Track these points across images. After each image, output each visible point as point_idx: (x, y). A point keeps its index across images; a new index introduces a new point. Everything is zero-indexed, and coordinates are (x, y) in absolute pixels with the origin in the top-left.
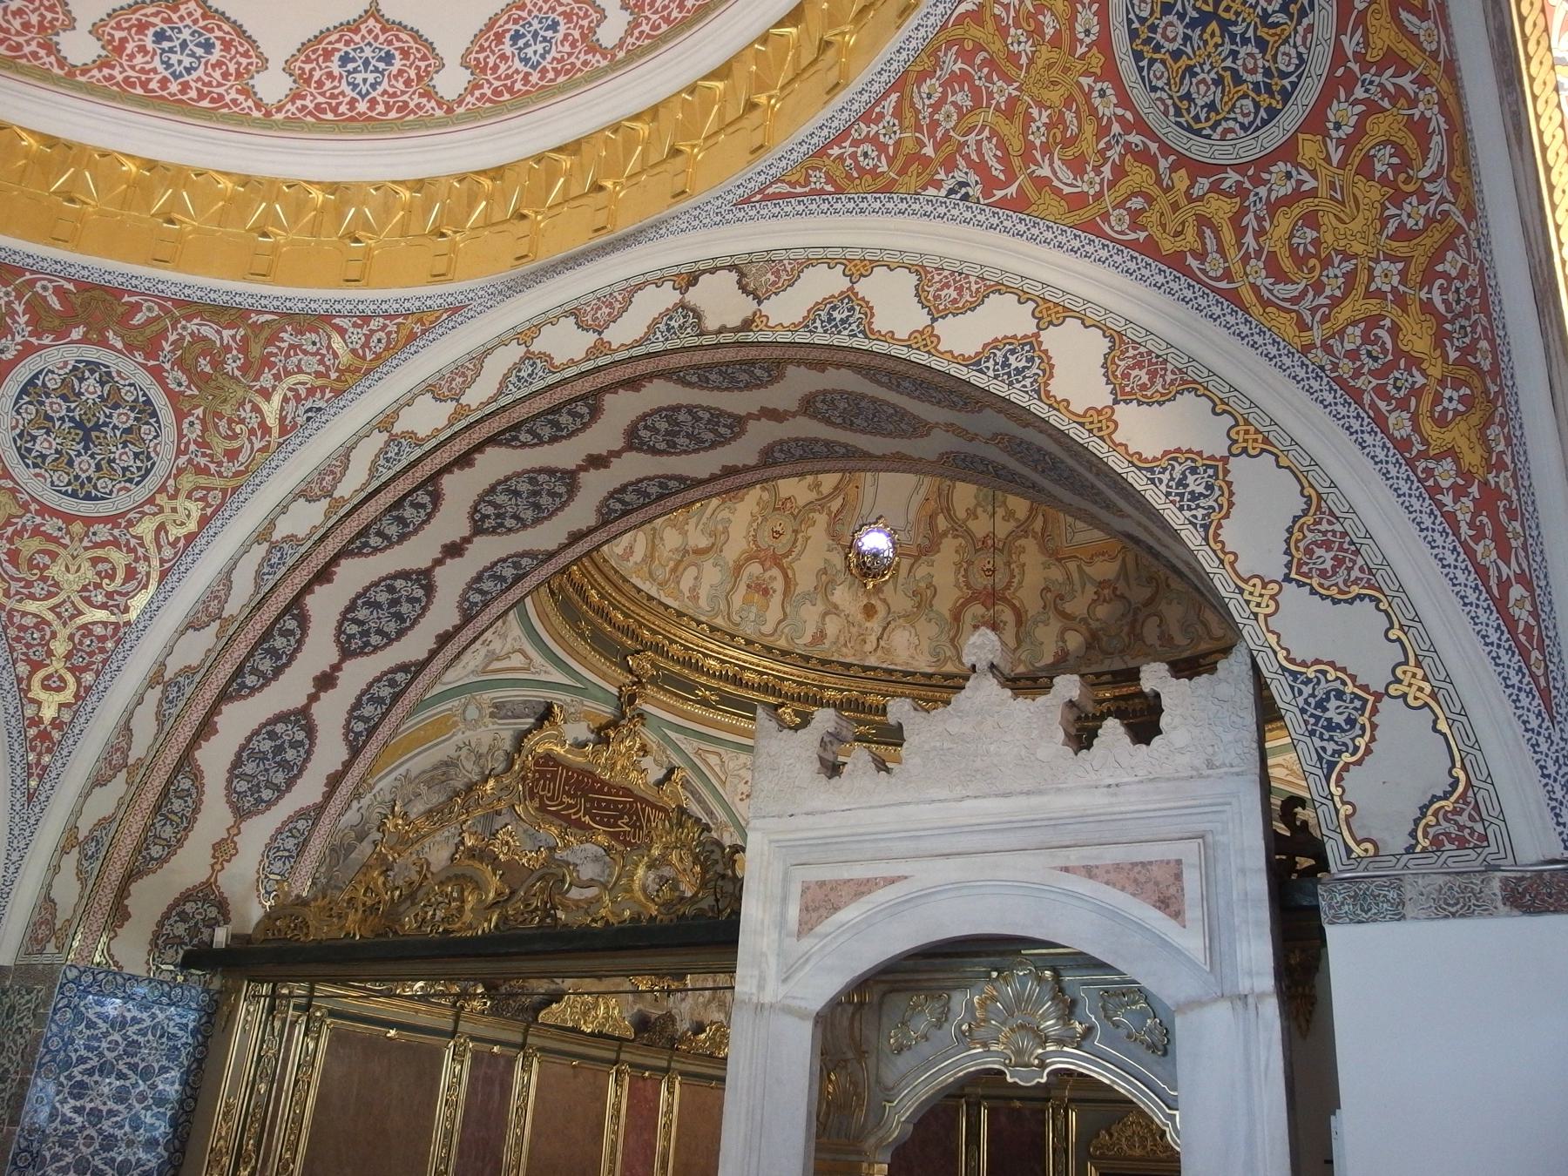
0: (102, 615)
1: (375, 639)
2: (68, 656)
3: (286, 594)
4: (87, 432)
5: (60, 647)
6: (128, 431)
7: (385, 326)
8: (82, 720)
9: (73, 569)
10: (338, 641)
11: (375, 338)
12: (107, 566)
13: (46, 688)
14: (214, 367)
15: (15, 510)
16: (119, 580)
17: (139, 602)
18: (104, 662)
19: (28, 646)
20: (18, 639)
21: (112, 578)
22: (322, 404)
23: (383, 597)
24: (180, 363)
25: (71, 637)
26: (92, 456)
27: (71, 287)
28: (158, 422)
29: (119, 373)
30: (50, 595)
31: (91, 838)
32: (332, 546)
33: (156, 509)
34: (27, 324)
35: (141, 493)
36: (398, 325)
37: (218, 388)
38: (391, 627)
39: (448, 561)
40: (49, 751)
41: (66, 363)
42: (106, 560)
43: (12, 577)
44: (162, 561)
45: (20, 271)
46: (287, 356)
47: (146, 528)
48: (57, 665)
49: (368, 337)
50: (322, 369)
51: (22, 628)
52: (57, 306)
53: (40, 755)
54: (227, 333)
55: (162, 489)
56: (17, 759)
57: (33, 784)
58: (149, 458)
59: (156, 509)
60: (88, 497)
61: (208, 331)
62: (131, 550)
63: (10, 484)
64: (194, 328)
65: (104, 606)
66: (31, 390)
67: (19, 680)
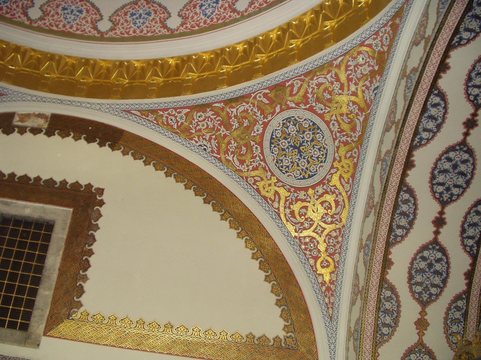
0: (333, 226)
1: (455, 191)
2: (327, 250)
3: (395, 181)
4: (298, 148)
5: (322, 247)
6: (312, 140)
7: (386, 30)
8: (340, 277)
9: (315, 211)
10: (435, 198)
11: (384, 39)
12: (327, 204)
13: (323, 267)
14: (331, 95)
15: (287, 194)
16: (334, 209)
17: (344, 215)
18: (340, 247)
19: (310, 251)
20: (306, 249)
21: (331, 208)
22: (377, 84)
23: (447, 166)
24: (318, 100)
25: (325, 241)
26: (304, 158)
27: (267, 91)
28: (321, 131)
29: (298, 117)
30: (311, 225)
31: (356, 330)
32: (404, 146)
33: (335, 170)
34: (261, 115)
35: (327, 166)
36: (391, 26)
37: (337, 103)
38: (461, 181)
39: (471, 131)
40: (332, 295)
41: (279, 124)
42: (326, 201)
43: (295, 223)
44: (347, 192)
45: (249, 96)
46: (355, 72)
47: (335, 180)
48: (323, 255)
49: (381, 41)
50: (371, 68)
51: (306, 244)
52: (267, 102)
53: (329, 298)
54: (328, 76)
55: (335, 160)
56: (322, 302)
57: (331, 312)
58: (324, 148)
59: (335, 170)
60: (310, 177)
61: (321, 80)
62: (333, 193)
63: (281, 184)
64: (316, 81)
65: (332, 223)
66: (273, 141)
67: (312, 267)
